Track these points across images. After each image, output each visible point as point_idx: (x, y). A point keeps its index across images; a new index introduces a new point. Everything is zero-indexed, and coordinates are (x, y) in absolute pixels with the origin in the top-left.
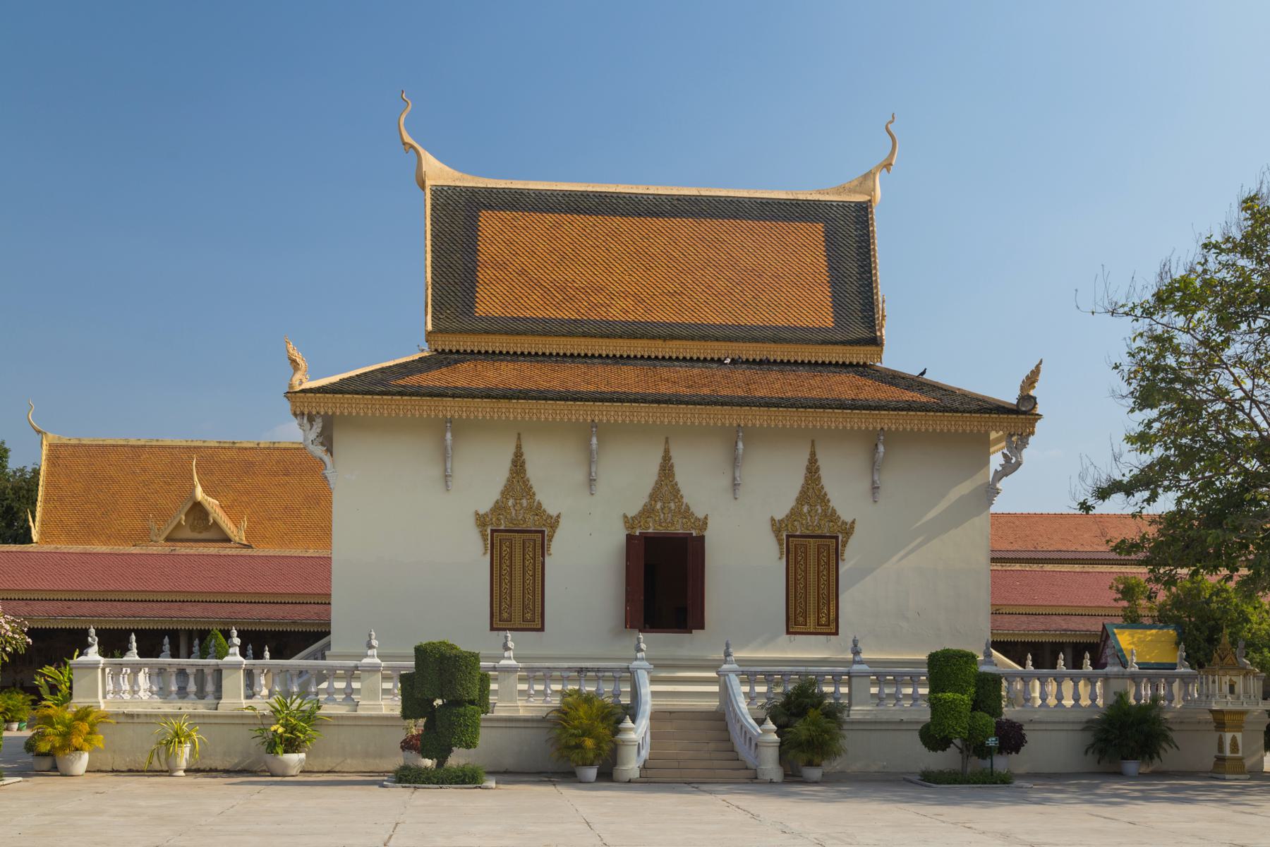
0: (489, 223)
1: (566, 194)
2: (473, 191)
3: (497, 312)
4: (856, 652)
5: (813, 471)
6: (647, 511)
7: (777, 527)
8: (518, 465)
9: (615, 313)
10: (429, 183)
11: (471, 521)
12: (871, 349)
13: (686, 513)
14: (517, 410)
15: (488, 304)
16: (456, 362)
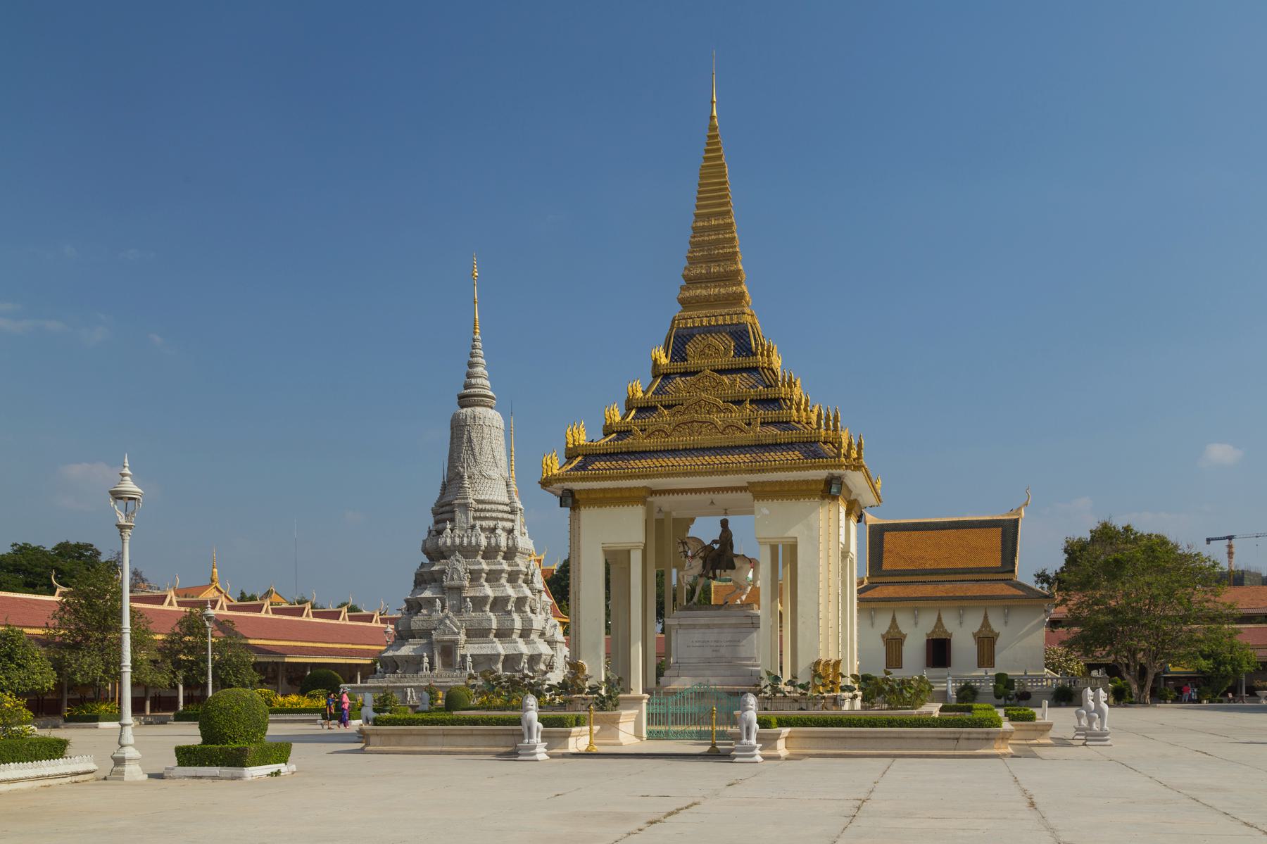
0: (888, 536)
1: (913, 524)
2: (882, 525)
3: (889, 568)
4: (986, 673)
5: (986, 618)
6: (933, 632)
7: (974, 635)
8: (894, 620)
9: (928, 566)
10: (868, 524)
11: (880, 636)
12: (1011, 574)
13: (946, 632)
14: (892, 605)
15: (886, 566)
16: (876, 587)
